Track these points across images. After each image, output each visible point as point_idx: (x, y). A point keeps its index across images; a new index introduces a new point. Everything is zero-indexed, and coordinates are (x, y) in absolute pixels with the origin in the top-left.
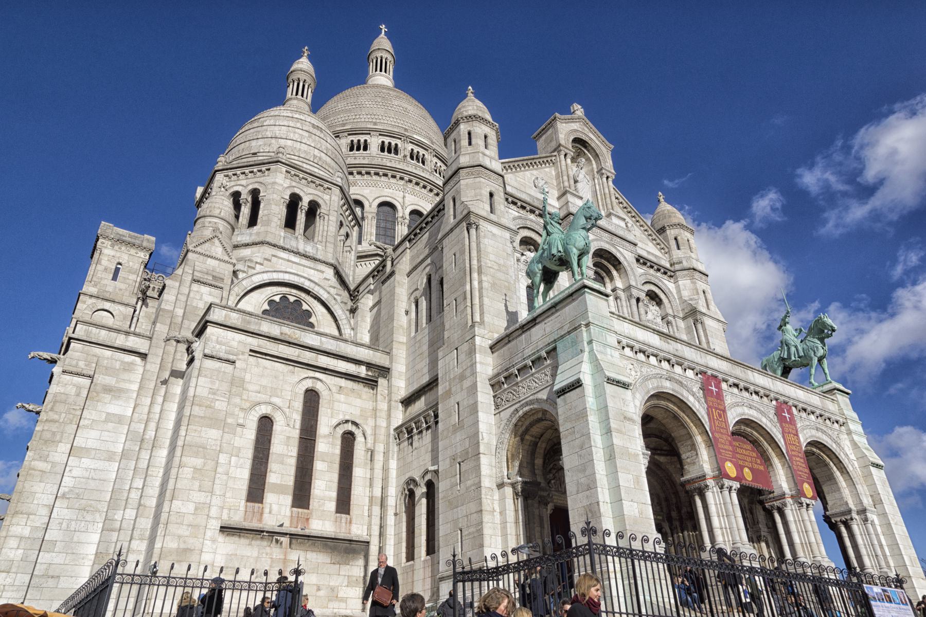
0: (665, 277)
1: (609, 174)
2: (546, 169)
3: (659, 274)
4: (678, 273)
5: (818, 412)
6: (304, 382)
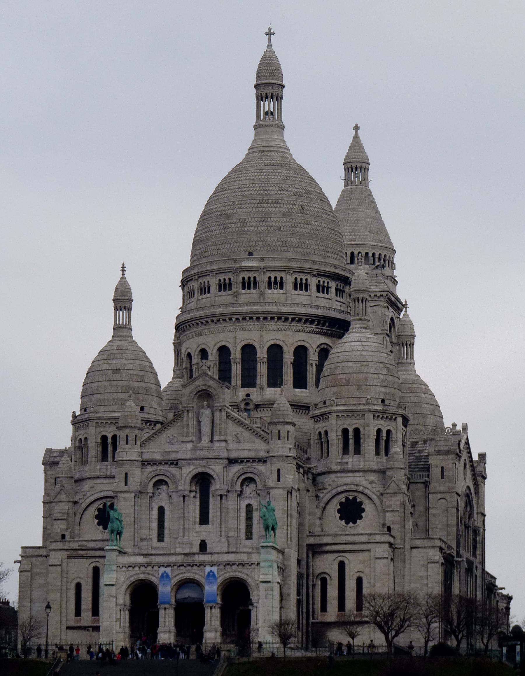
0: (261, 464)
1: (220, 408)
2: (178, 425)
3: (254, 464)
4: (268, 459)
5: (237, 564)
6: (92, 564)
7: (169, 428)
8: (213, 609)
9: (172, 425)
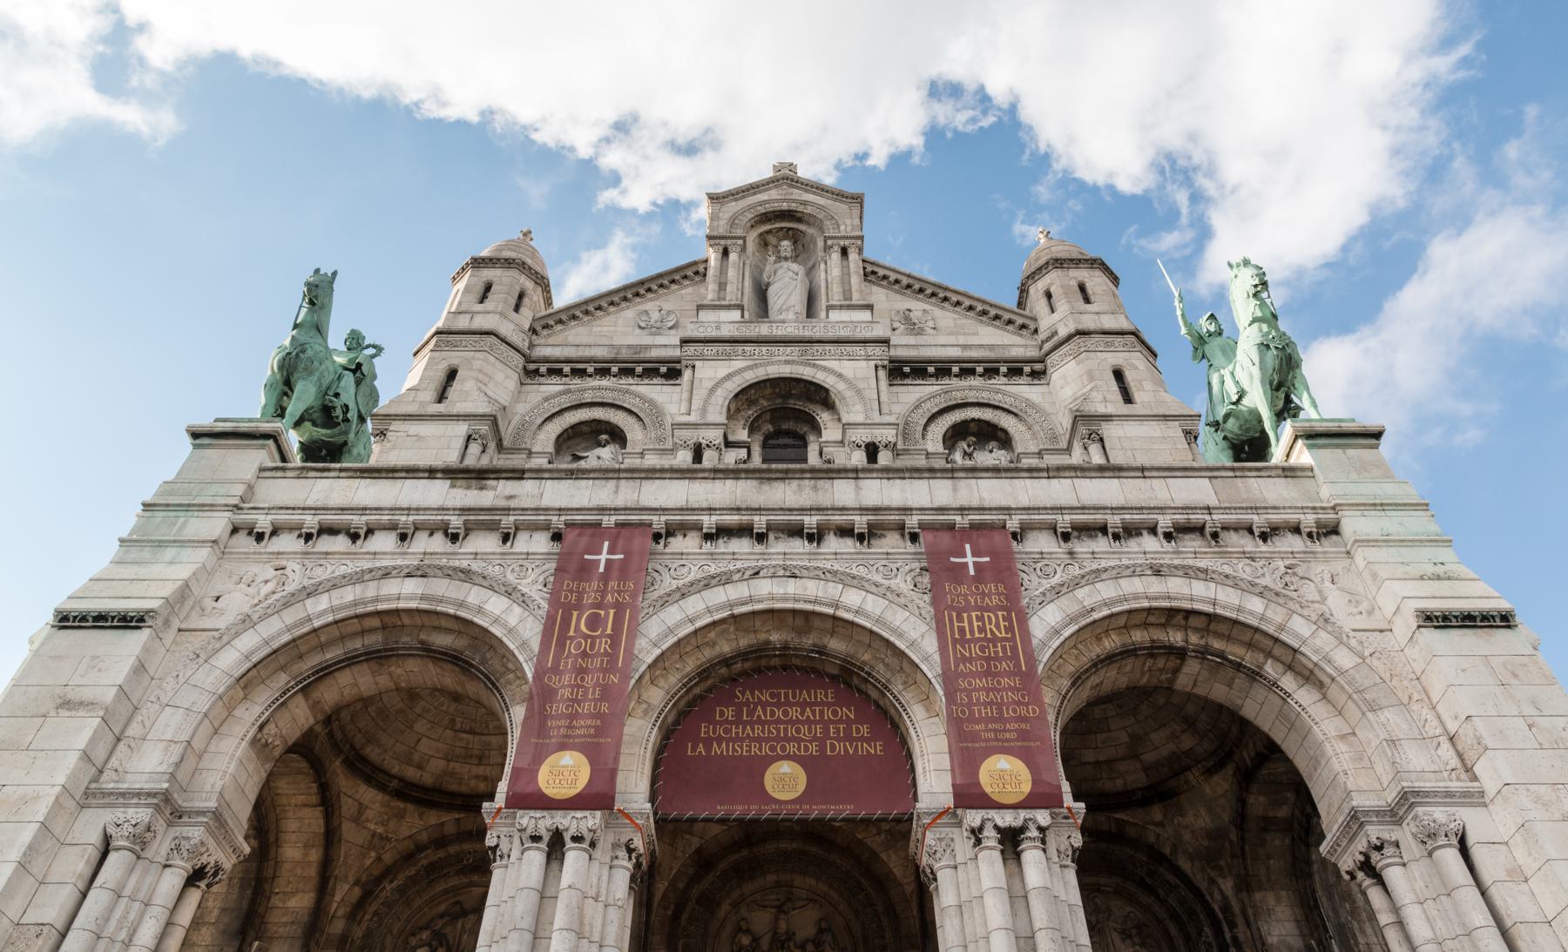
0: (1017, 380)
1: (842, 243)
2: (683, 292)
4: (1048, 362)
5: (1165, 522)
7: (650, 295)
8: (1032, 857)
9: (661, 291)
